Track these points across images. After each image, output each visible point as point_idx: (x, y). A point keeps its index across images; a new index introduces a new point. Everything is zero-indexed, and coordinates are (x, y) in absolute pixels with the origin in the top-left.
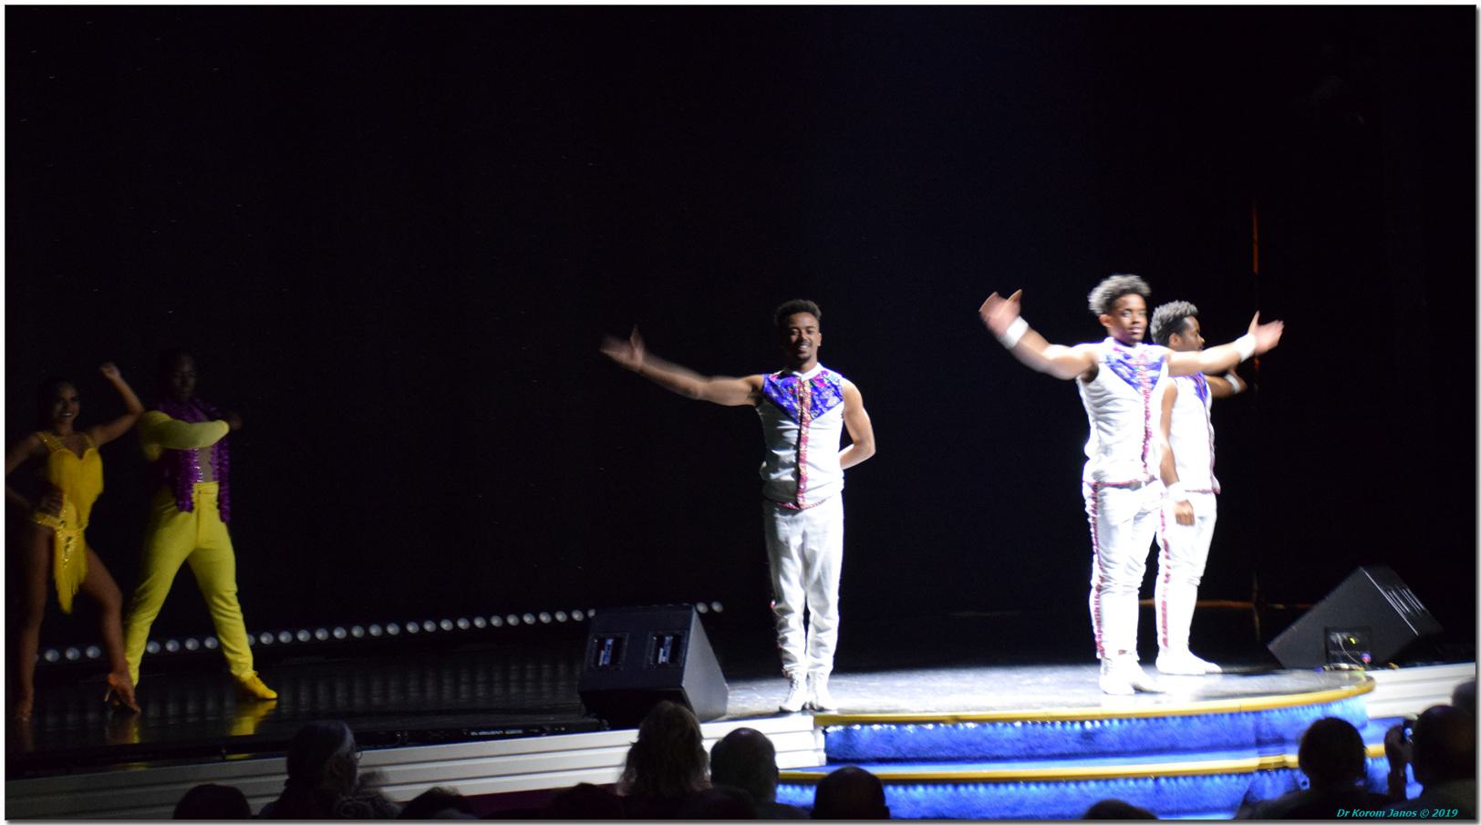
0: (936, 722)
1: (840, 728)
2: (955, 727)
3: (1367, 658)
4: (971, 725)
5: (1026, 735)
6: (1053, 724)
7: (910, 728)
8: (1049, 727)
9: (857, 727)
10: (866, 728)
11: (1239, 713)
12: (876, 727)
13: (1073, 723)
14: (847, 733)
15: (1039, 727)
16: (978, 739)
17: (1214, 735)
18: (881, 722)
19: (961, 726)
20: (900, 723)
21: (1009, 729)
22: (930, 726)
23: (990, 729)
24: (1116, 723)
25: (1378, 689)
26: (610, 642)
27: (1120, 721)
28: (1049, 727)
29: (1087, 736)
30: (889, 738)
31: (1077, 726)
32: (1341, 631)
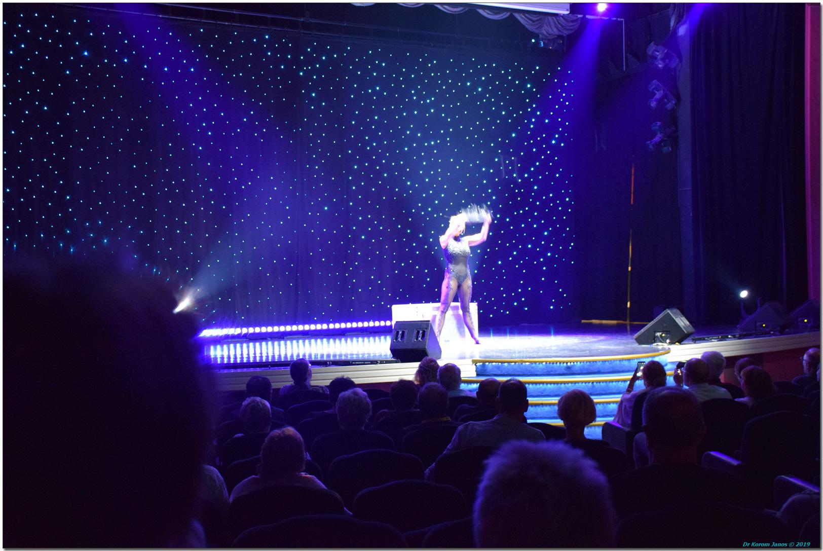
0: (515, 362)
3: (668, 341)
14: (484, 365)
20: (502, 362)
29: (568, 368)
30: (498, 368)
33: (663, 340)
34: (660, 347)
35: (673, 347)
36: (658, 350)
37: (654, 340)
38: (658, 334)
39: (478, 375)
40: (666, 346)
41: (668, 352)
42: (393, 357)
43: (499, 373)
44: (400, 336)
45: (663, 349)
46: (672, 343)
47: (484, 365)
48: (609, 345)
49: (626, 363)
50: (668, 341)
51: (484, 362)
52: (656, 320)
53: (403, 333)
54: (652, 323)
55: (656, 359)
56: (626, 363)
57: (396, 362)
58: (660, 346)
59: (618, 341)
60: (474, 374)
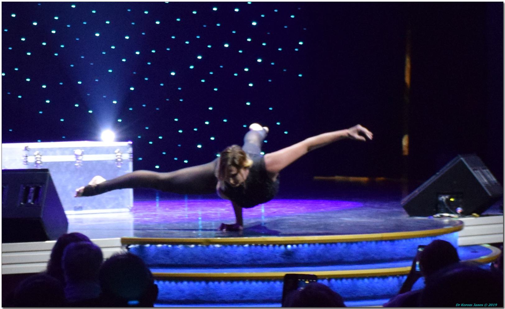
0: (196, 243)
1: (137, 246)
2: (208, 246)
3: (459, 210)
4: (218, 246)
6: (268, 246)
7: (180, 246)
8: (265, 248)
9: (148, 245)
10: (153, 246)
12: (159, 246)
13: (280, 245)
15: (259, 248)
16: (222, 255)
17: (365, 254)
18: (162, 243)
19: (211, 246)
21: (241, 249)
22: (193, 246)
23: (229, 248)
24: (306, 246)
25: (465, 229)
27: (309, 244)
28: (265, 248)
29: (288, 254)
30: (167, 253)
31: (282, 247)
32: (444, 194)
33: (451, 208)
34: (446, 221)
35: (467, 220)
36: (439, 225)
37: (437, 208)
38: (443, 198)
40: (455, 218)
41: (459, 227)
43: (169, 262)
45: (450, 224)
46: (465, 214)
47: (141, 248)
48: (360, 216)
49: (387, 247)
50: (459, 210)
51: (142, 243)
52: (439, 174)
54: (433, 178)
55: (441, 238)
56: (387, 247)
58: (447, 218)
59: (374, 210)
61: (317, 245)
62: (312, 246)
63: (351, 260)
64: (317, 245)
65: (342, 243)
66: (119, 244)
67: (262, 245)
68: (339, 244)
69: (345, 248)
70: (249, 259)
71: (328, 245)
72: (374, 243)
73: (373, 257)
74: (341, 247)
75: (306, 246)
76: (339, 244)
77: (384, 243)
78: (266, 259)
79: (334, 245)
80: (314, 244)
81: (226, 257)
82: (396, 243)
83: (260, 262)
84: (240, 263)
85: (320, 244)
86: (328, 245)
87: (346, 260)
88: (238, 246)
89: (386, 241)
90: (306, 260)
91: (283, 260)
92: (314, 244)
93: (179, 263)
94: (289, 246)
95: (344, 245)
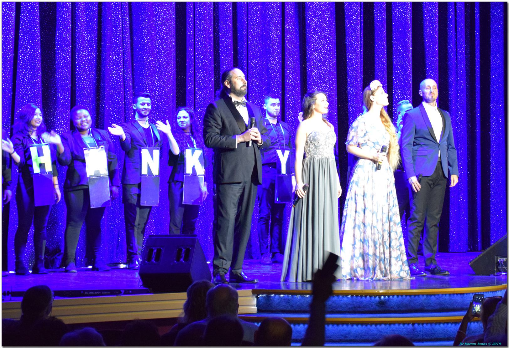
1: (265, 295)
5: (353, 302)
6: (366, 296)
8: (364, 298)
9: (273, 295)
10: (277, 295)
11: (454, 294)
12: (282, 295)
14: (268, 298)
15: (359, 298)
21: (345, 298)
24: (395, 297)
26: (155, 251)
27: (398, 296)
28: (364, 298)
29: (382, 303)
30: (287, 301)
31: (377, 298)
39: (259, 311)
42: (144, 285)
43: (289, 308)
44: (154, 256)
49: (458, 298)
53: (159, 251)
57: (147, 292)
60: (253, 309)
61: (404, 297)
62: (400, 297)
63: (430, 308)
64: (404, 297)
65: (423, 295)
66: (251, 294)
67: (361, 296)
68: (421, 296)
69: (425, 299)
70: (351, 306)
71: (413, 297)
72: (448, 296)
73: (447, 307)
74: (423, 298)
75: (395, 297)
76: (421, 296)
77: (455, 295)
78: (364, 307)
79: (417, 297)
80: (402, 296)
81: (334, 305)
82: (465, 295)
83: (360, 309)
84: (345, 310)
85: (406, 296)
86: (413, 297)
87: (426, 308)
88: (343, 297)
89: (457, 294)
90: (396, 308)
91: (377, 308)
92: (402, 296)
93: (297, 310)
94: (382, 297)
95: (425, 297)
